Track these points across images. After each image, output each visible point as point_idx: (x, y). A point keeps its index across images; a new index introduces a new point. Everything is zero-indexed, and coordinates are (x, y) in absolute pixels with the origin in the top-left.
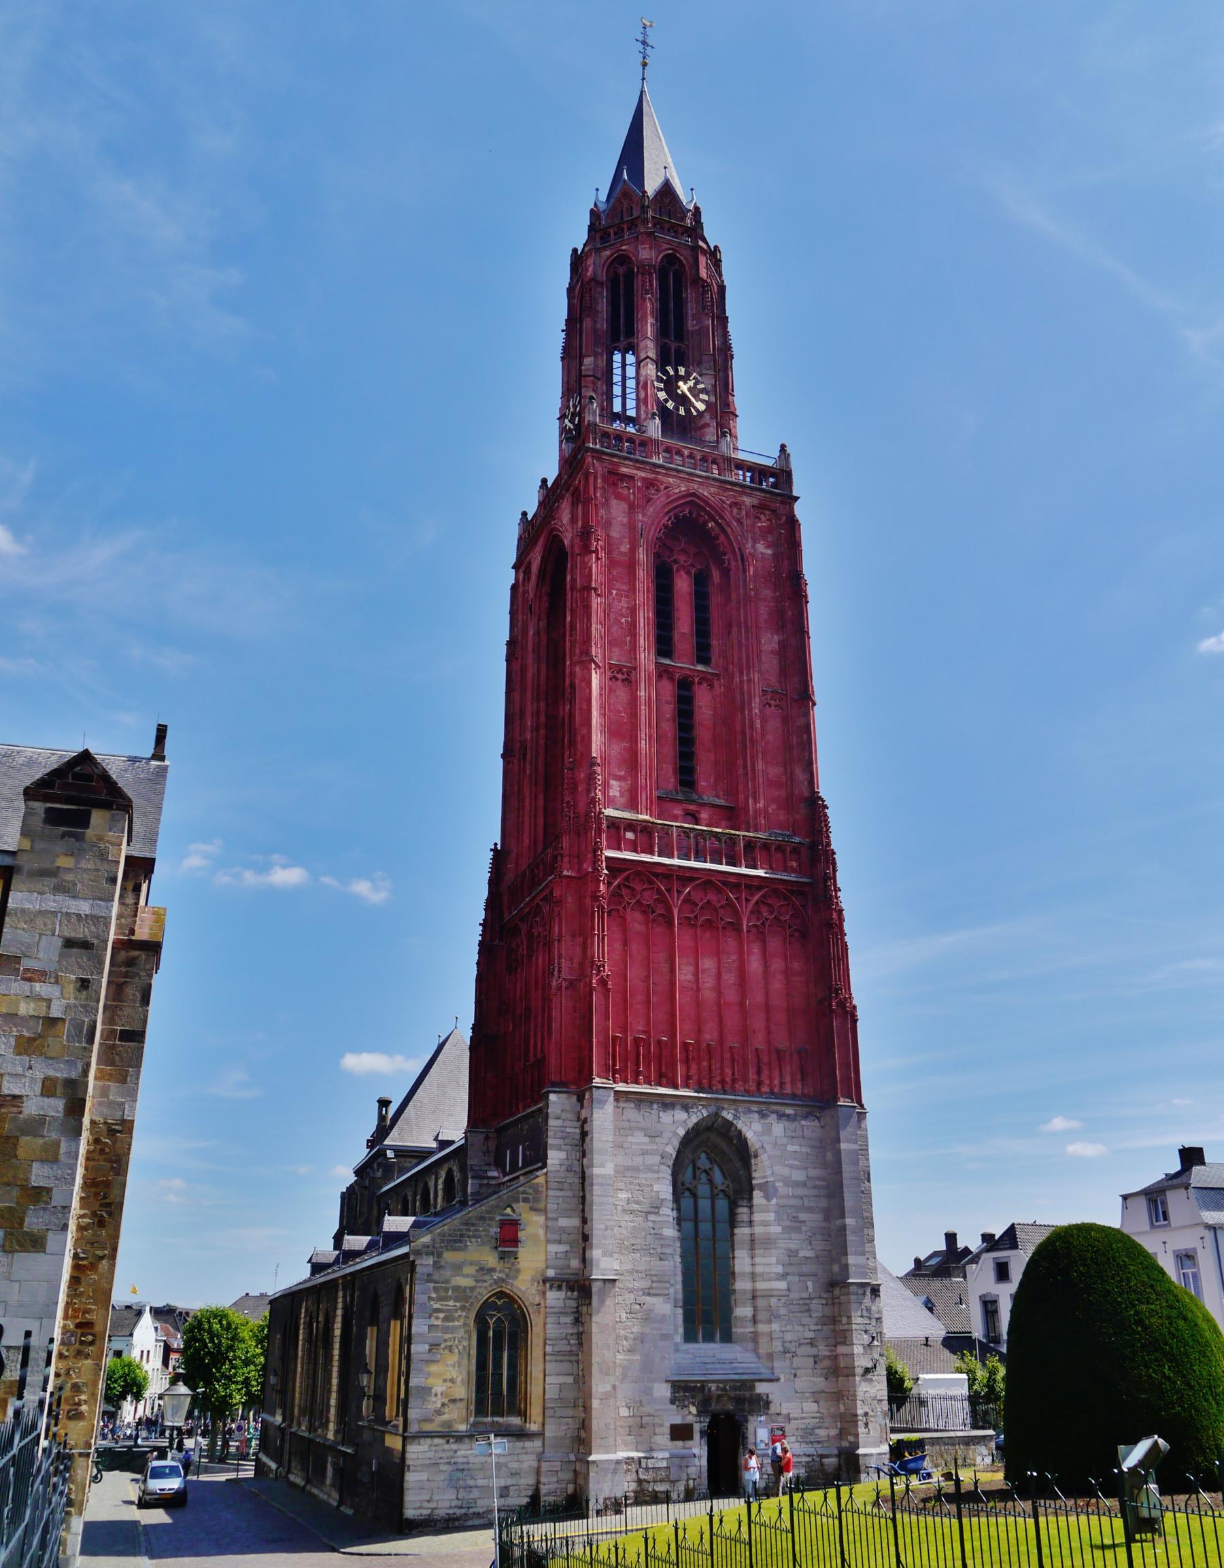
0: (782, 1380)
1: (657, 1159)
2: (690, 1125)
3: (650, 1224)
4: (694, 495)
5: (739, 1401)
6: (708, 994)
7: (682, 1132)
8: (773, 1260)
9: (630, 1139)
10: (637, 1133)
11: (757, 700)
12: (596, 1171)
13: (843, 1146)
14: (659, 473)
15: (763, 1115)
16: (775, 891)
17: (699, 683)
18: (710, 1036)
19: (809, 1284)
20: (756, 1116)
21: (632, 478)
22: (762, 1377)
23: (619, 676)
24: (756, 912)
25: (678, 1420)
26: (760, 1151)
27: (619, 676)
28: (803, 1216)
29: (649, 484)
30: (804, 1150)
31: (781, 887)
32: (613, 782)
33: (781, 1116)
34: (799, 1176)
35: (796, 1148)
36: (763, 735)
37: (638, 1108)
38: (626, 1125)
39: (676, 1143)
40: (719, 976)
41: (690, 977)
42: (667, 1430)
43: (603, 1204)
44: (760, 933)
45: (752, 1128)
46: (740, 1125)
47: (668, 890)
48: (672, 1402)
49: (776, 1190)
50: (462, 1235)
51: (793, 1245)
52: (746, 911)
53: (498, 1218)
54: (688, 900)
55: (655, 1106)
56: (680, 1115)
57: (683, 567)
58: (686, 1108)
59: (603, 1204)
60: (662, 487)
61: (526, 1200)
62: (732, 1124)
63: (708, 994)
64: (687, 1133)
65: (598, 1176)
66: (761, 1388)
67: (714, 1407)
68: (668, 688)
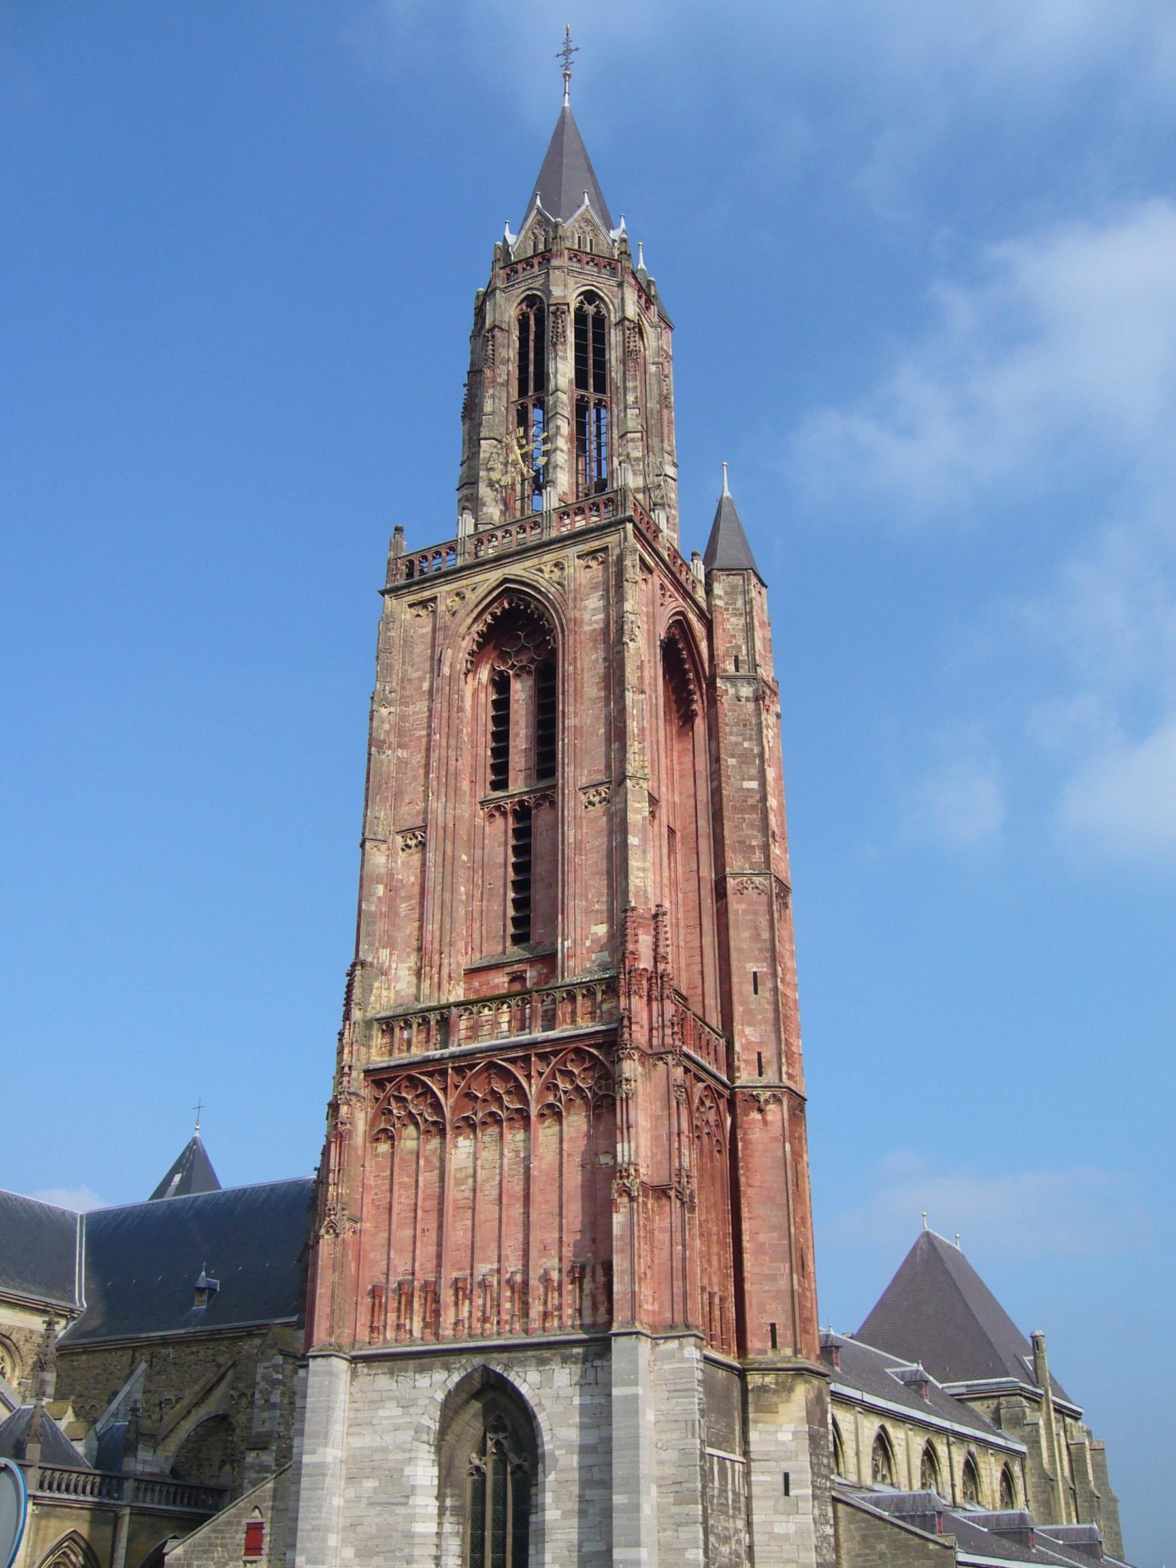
1: (412, 1433)
4: (506, 580)
7: (440, 1396)
9: (381, 1413)
10: (388, 1405)
12: (306, 1459)
13: (616, 1391)
16: (578, 1051)
17: (538, 805)
23: (413, 843)
27: (413, 843)
30: (596, 1400)
33: (565, 1360)
37: (391, 1372)
38: (377, 1396)
43: (310, 1499)
44: (554, 1113)
46: (512, 1377)
49: (556, 1460)
50: (211, 1545)
52: (533, 1089)
53: (245, 1521)
56: (439, 1376)
59: (310, 1499)
62: (500, 1376)
65: (308, 1465)
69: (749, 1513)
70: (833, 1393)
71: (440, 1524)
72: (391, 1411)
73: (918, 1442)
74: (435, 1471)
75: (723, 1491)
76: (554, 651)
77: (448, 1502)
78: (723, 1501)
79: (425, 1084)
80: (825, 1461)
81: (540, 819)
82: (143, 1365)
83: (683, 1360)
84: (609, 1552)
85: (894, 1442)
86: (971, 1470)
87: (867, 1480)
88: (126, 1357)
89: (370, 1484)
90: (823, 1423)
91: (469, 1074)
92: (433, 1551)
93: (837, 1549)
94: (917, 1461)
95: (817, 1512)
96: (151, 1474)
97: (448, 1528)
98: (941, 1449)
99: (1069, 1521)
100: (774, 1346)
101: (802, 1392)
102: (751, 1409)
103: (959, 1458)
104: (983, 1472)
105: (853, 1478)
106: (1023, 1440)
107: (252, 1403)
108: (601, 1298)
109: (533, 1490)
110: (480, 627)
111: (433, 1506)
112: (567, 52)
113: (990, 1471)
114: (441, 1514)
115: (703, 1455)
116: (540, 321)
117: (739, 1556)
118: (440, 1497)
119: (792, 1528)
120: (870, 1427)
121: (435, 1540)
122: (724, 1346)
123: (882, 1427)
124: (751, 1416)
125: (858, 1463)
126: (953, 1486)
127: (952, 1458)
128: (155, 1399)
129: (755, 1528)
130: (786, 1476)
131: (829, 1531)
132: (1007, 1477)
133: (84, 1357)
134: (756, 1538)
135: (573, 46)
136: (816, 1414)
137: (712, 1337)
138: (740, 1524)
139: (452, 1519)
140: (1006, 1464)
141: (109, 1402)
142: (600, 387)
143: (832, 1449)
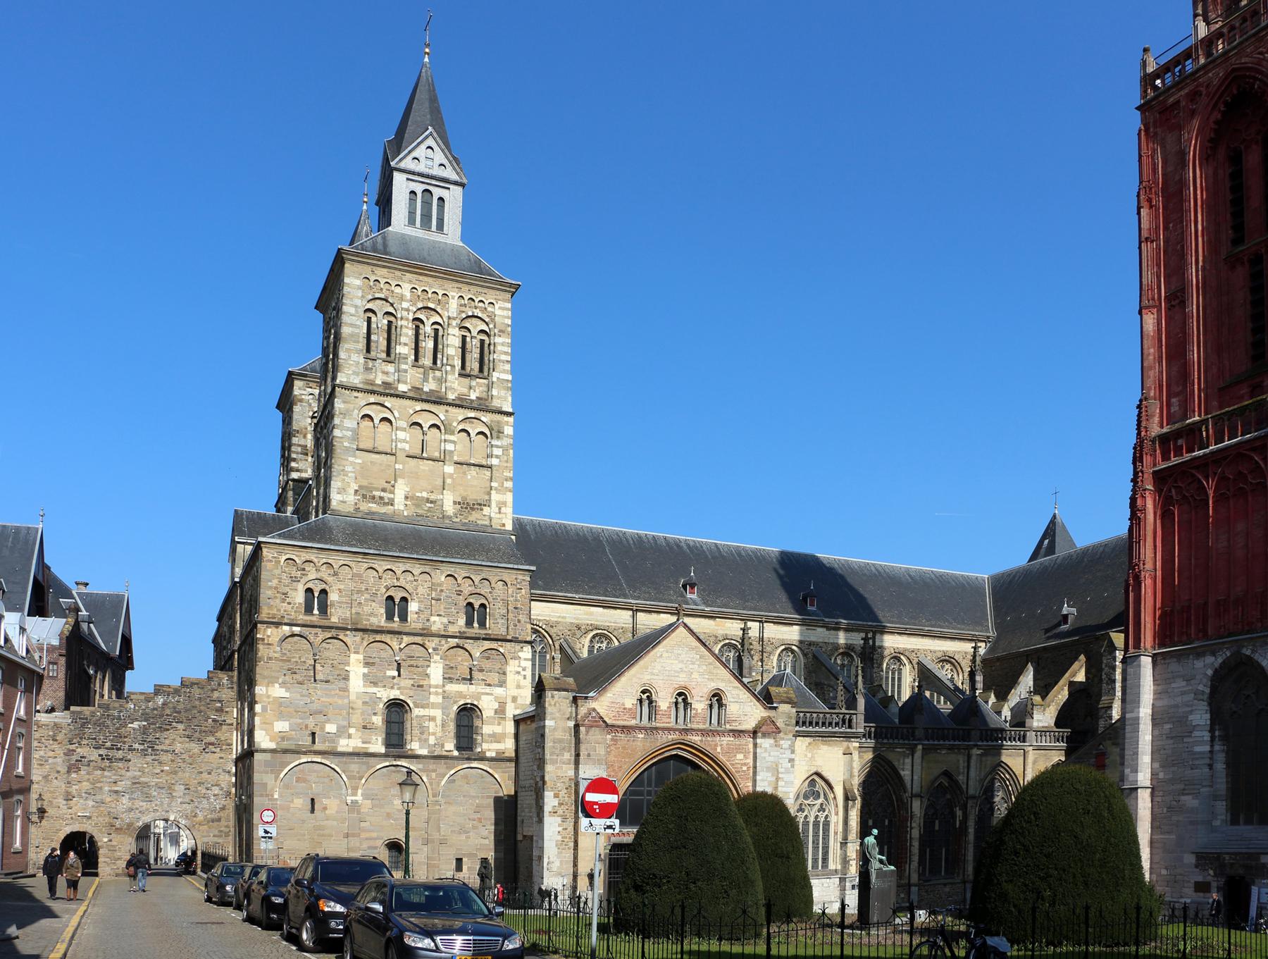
2: (1217, 665)
7: (1210, 672)
25: (1200, 879)
32: (1174, 400)
42: (1192, 885)
48: (1196, 867)
56: (1209, 659)
58: (1214, 654)
64: (1216, 671)
71: (1212, 746)
74: (1208, 716)
77: (1217, 733)
79: (1193, 476)
92: (1208, 761)
97: (1217, 748)
111: (1207, 736)
114: (1213, 739)
118: (1212, 731)
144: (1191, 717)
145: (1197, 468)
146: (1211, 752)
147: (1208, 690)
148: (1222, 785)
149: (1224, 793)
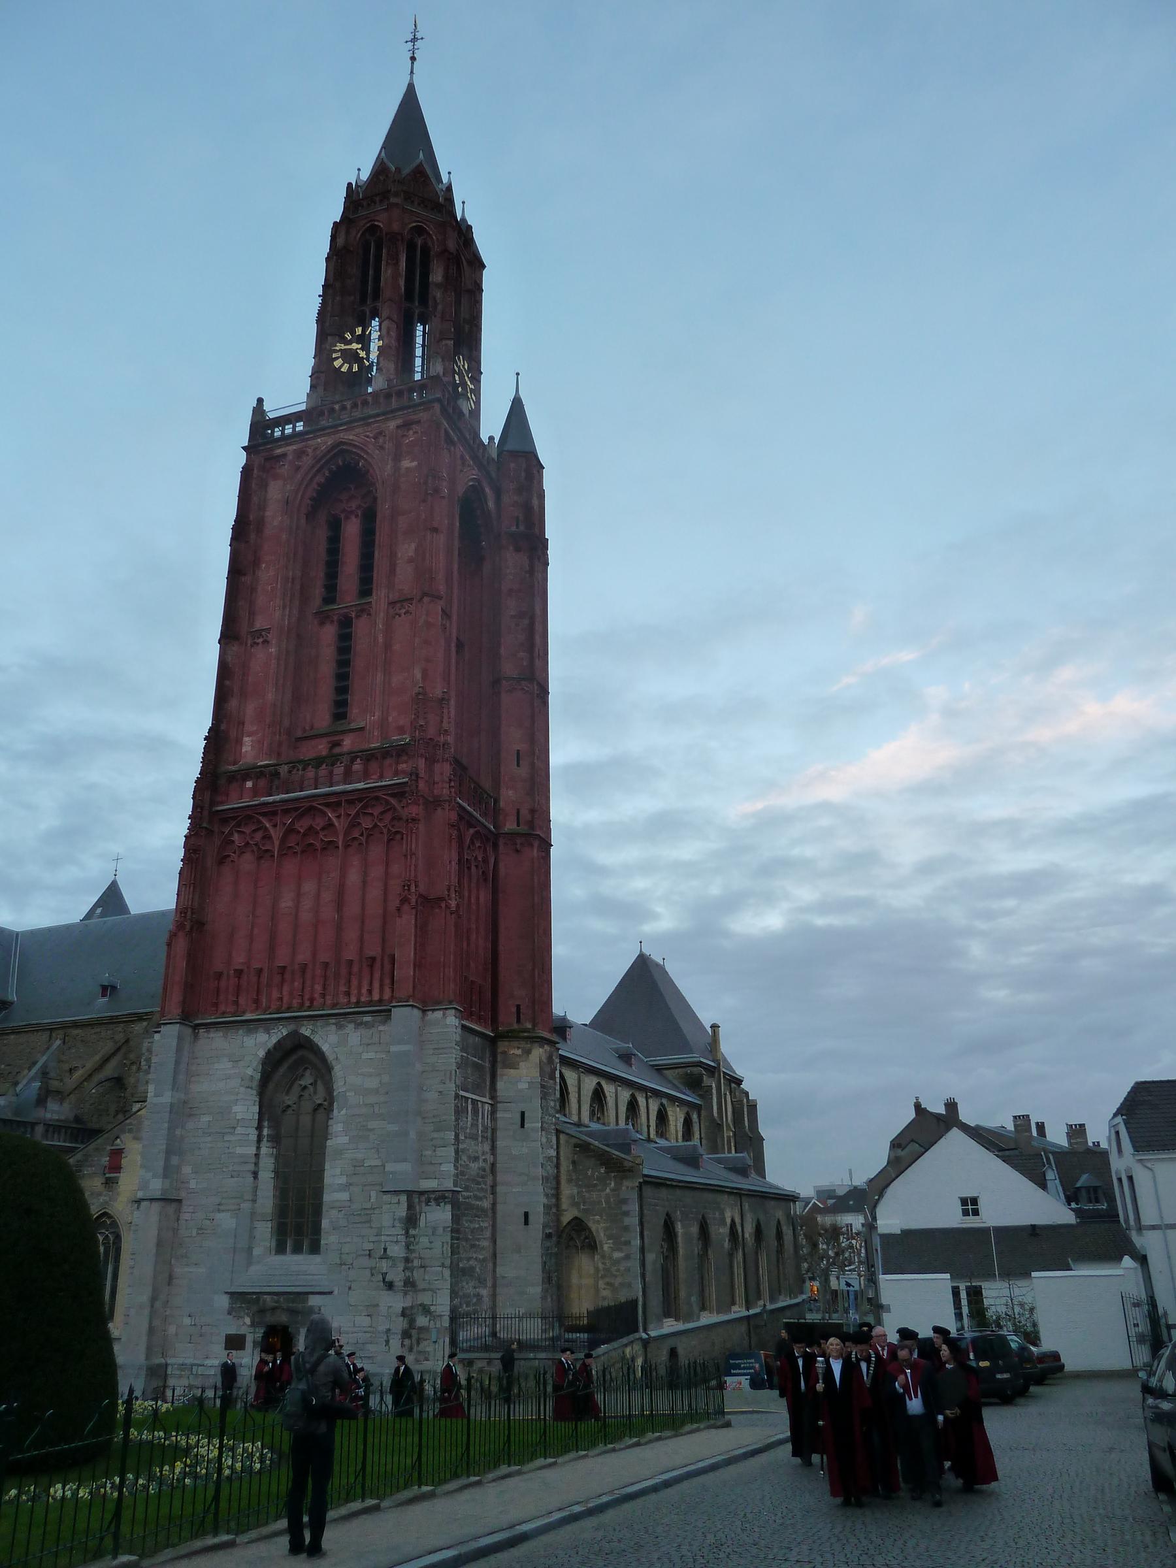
0: (336, 1292)
2: (270, 1045)
3: (227, 1145)
5: (293, 1312)
6: (306, 916)
7: (262, 1053)
8: (338, 1171)
9: (216, 1066)
11: (382, 614)
14: (308, 439)
15: (340, 1027)
17: (358, 617)
18: (303, 956)
19: (373, 1194)
20: (334, 1027)
21: (284, 455)
22: (317, 1289)
24: (354, 824)
25: (232, 1331)
26: (334, 1063)
28: (372, 1124)
29: (300, 454)
31: (379, 794)
33: (359, 1025)
34: (372, 1083)
35: (371, 1055)
36: (388, 646)
39: (255, 1064)
40: (318, 896)
41: (290, 904)
45: (327, 1039)
46: (316, 1039)
47: (275, 826)
48: (229, 1313)
51: (360, 1156)
53: (109, 1148)
54: (290, 831)
55: (241, 1032)
57: (352, 512)
58: (268, 1031)
60: (310, 451)
61: (130, 1131)
63: (306, 916)
66: (314, 1301)
67: (270, 1319)
68: (329, 633)
69: (493, 1141)
70: (562, 1058)
71: (258, 1148)
72: (224, 1066)
73: (625, 1095)
75: (474, 1125)
76: (375, 499)
77: (265, 1132)
78: (474, 1131)
79: (259, 822)
80: (552, 1104)
81: (361, 628)
82: (58, 1042)
83: (446, 1026)
84: (384, 1166)
85: (607, 1094)
86: (662, 1117)
87: (585, 1118)
88: (45, 1036)
89: (206, 1119)
90: (553, 1077)
91: (294, 814)
93: (558, 1166)
94: (623, 1109)
95: (544, 1140)
96: (58, 1120)
97: (264, 1150)
98: (641, 1100)
99: (730, 1152)
100: (518, 1021)
101: (538, 1053)
102: (499, 1065)
103: (654, 1107)
104: (671, 1118)
105: (575, 1118)
106: (701, 1096)
107: (139, 1069)
108: (387, 981)
109: (330, 1122)
110: (320, 479)
112: (414, 40)
113: (676, 1117)
114: (259, 1140)
115: (457, 1096)
116: (379, 248)
117: (484, 1170)
118: (259, 1128)
119: (525, 1150)
120: (590, 1083)
121: (253, 1160)
122: (480, 1019)
123: (599, 1084)
124: (499, 1071)
125: (580, 1108)
126: (648, 1126)
127: (649, 1108)
128: (66, 1067)
129: (499, 1151)
130: (523, 1114)
131: (554, 1154)
132: (688, 1123)
133: (12, 1037)
134: (499, 1158)
135: (418, 35)
136: (547, 1070)
137: (471, 1014)
138: (487, 1147)
139: (269, 1144)
140: (687, 1113)
141: (30, 1069)
142: (424, 300)
143: (558, 1095)
144: (235, 1109)
145: (264, 814)
146: (257, 1155)
147: (258, 1076)
148: (267, 1200)
149: (270, 1211)
